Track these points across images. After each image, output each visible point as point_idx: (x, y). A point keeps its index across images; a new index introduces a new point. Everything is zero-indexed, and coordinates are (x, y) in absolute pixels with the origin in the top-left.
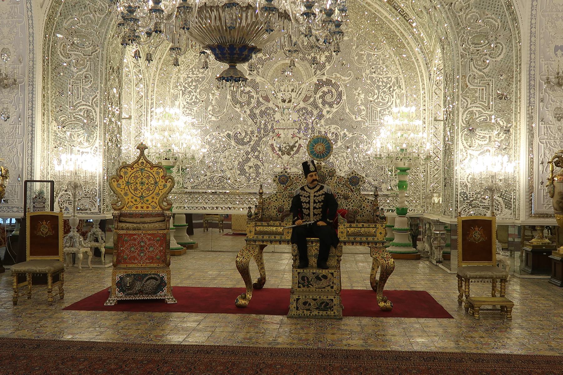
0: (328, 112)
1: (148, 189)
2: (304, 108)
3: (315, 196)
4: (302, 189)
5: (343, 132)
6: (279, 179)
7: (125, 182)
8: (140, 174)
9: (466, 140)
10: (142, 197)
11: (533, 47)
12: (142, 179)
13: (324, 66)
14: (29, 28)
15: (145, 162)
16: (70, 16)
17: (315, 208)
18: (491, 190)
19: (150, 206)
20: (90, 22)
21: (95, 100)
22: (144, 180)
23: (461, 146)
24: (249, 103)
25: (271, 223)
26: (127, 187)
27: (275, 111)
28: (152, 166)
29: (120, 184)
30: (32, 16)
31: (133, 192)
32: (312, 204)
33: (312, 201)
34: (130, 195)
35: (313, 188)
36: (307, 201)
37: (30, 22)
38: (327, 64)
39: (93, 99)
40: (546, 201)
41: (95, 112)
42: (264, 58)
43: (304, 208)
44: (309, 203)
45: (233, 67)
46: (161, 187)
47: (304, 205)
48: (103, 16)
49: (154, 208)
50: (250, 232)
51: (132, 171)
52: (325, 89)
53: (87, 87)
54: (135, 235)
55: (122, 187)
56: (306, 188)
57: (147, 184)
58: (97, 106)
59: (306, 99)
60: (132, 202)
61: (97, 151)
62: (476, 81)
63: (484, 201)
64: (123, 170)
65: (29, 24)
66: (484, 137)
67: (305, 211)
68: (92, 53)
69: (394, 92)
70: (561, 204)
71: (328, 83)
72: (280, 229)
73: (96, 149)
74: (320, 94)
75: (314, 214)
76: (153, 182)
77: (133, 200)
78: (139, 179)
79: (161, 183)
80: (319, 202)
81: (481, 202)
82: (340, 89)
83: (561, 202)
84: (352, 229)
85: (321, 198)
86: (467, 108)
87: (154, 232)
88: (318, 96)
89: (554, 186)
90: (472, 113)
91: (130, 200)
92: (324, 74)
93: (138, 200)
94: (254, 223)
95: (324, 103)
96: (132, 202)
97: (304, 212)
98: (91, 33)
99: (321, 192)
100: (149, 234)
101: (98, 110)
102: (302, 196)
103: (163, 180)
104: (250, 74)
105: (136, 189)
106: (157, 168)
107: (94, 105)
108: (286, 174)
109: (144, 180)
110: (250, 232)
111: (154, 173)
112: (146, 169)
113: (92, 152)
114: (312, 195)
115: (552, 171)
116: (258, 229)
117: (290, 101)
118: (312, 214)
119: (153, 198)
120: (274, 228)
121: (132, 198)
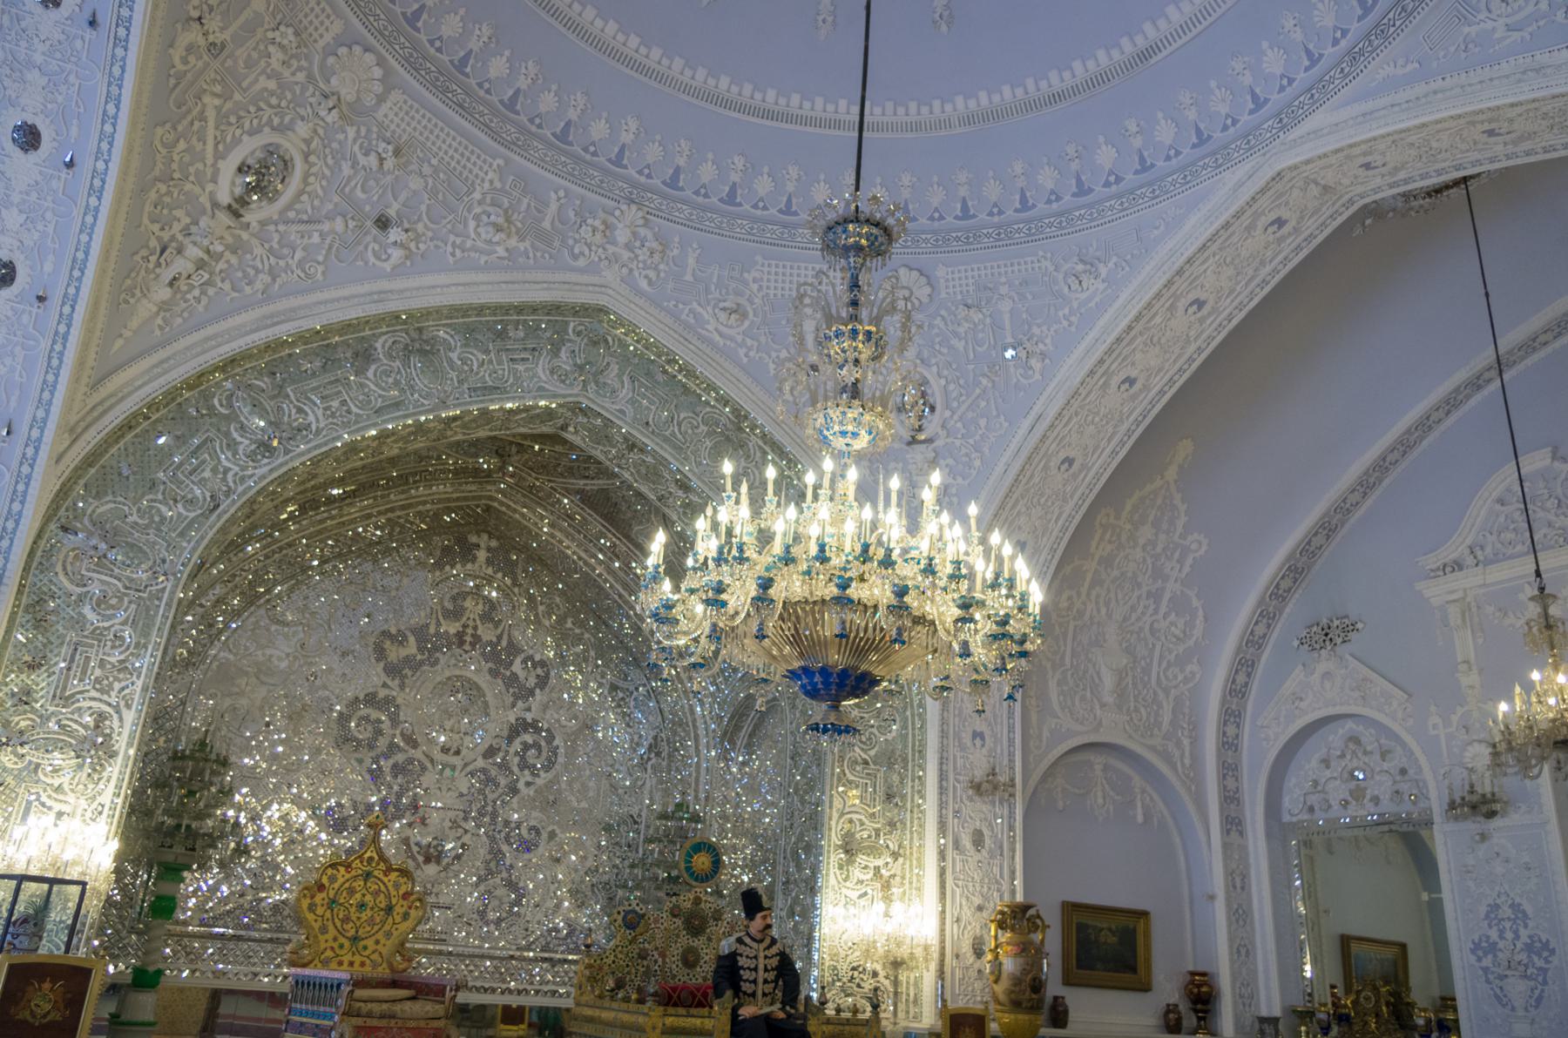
0: (528, 784)
1: (371, 921)
2: (483, 770)
3: (766, 957)
4: (740, 941)
5: (550, 829)
6: (624, 919)
7: (327, 900)
8: (362, 883)
9: (841, 867)
10: (355, 939)
11: (945, 727)
12: (364, 895)
13: (532, 693)
14: (12, 501)
15: (376, 858)
16: (110, 498)
17: (766, 981)
18: (897, 964)
19: (368, 962)
20: (157, 519)
21: (127, 691)
22: (368, 898)
23: (832, 881)
24: (371, 747)
25: (693, 1011)
26: (328, 914)
27: (424, 769)
28: (389, 870)
29: (316, 905)
30: (29, 477)
31: (338, 924)
32: (761, 972)
33: (761, 967)
34: (332, 932)
35: (762, 941)
36: (753, 966)
37: (21, 487)
38: (538, 691)
39: (123, 689)
40: (962, 988)
41: (121, 719)
42: (419, 657)
43: (745, 981)
44: (756, 969)
45: (836, 707)
46: (398, 919)
47: (746, 975)
48: (192, 515)
49: (375, 965)
50: (654, 1028)
51: (348, 876)
52: (529, 738)
53: (113, 660)
54: (379, 1029)
55: (320, 911)
56: (747, 940)
57: (372, 909)
58: (128, 707)
59: (490, 752)
60: (332, 948)
61: (100, 813)
62: (858, 768)
63: (863, 984)
64: (330, 871)
65: (15, 491)
66: (866, 867)
67: (746, 987)
68: (146, 587)
69: (650, 763)
70: (1013, 996)
71: (534, 726)
72: (709, 1024)
73: (100, 808)
74: (517, 745)
75: (764, 995)
76: (383, 906)
77: (336, 945)
78: (358, 896)
79: (399, 910)
80: (773, 969)
81: (859, 986)
82: (556, 743)
83: (1012, 992)
84: (831, 1027)
85: (775, 962)
86: (842, 814)
87: (422, 1024)
88: (512, 750)
89: (1000, 964)
90: (851, 821)
91: (331, 943)
92: (529, 709)
93: (347, 944)
94: (662, 1008)
95: (524, 765)
96: (332, 948)
97: (743, 989)
98: (155, 543)
99: (774, 950)
100: (408, 1029)
101: (130, 716)
102: (741, 955)
103: (405, 903)
104: (385, 685)
105: (346, 920)
106: (397, 874)
107: (122, 703)
108: (638, 909)
109: (368, 898)
110: (654, 1028)
111: (390, 885)
112: (376, 873)
113: (89, 814)
114: (762, 955)
115: (996, 937)
116: (669, 1021)
117: (458, 753)
118: (760, 993)
119: (377, 942)
120: (698, 1022)
121: (335, 939)
